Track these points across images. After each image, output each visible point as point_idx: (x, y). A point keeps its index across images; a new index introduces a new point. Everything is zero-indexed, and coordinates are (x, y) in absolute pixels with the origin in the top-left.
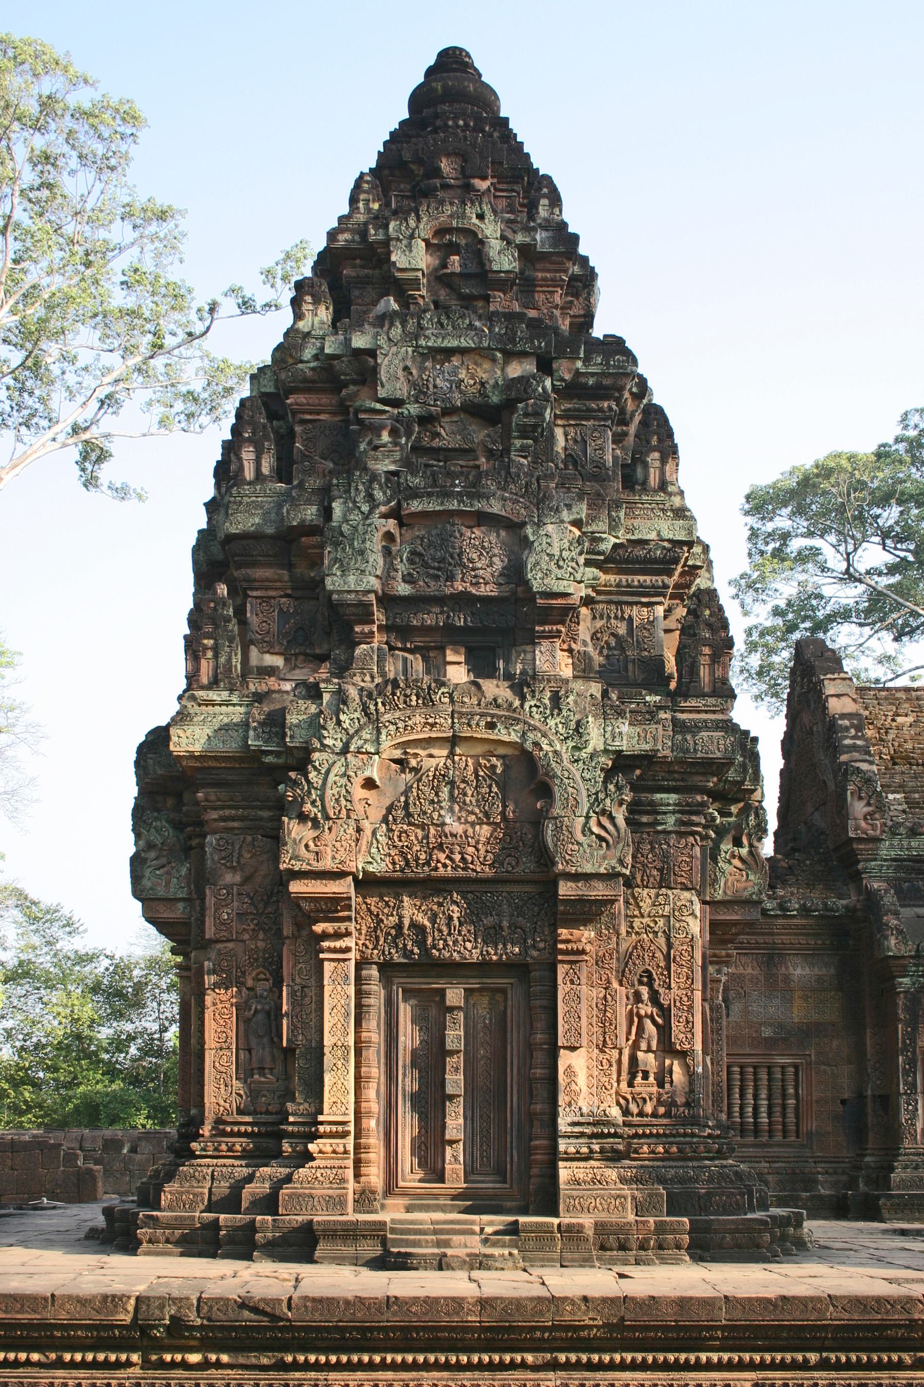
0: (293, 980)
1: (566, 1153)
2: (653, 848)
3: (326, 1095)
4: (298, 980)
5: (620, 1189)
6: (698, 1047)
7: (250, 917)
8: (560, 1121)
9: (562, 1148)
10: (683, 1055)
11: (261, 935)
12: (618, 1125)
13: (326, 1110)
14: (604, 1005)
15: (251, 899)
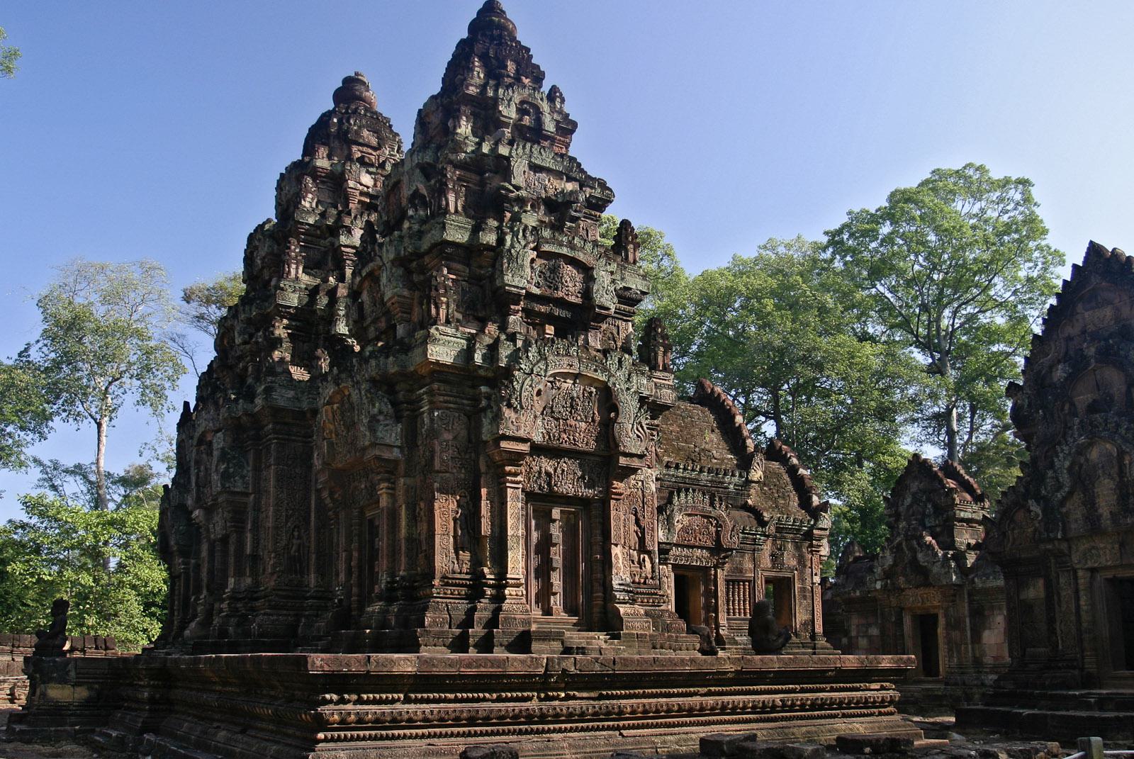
10: (649, 553)
11: (463, 471)
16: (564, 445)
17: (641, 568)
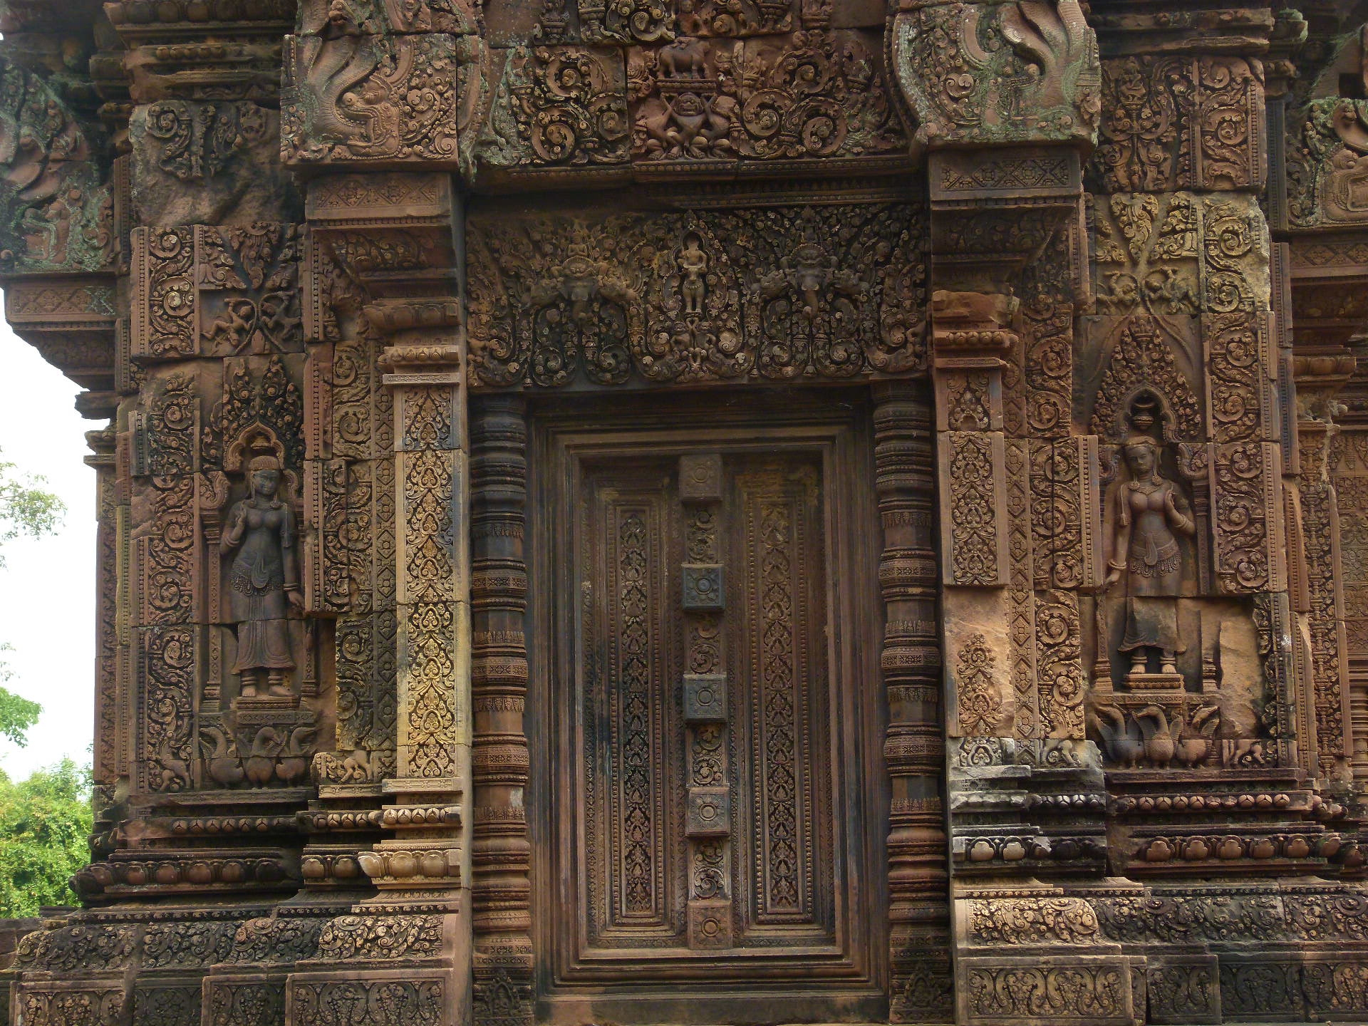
0: (327, 445)
1: (968, 857)
2: (1151, 95)
3: (403, 727)
4: (339, 447)
5: (1106, 950)
6: (1279, 582)
7: (233, 300)
8: (952, 777)
9: (958, 844)
12: (1093, 787)
13: (402, 765)
14: (1049, 486)
15: (236, 254)
16: (659, 158)
17: (1194, 684)
